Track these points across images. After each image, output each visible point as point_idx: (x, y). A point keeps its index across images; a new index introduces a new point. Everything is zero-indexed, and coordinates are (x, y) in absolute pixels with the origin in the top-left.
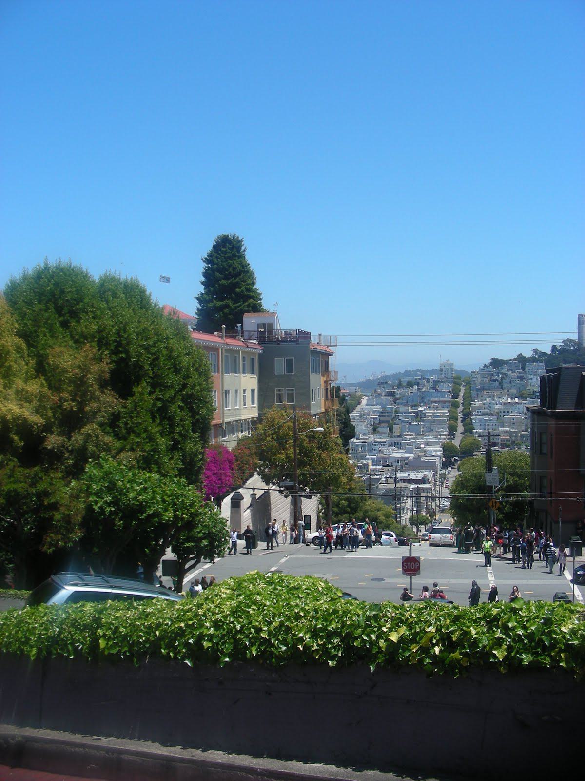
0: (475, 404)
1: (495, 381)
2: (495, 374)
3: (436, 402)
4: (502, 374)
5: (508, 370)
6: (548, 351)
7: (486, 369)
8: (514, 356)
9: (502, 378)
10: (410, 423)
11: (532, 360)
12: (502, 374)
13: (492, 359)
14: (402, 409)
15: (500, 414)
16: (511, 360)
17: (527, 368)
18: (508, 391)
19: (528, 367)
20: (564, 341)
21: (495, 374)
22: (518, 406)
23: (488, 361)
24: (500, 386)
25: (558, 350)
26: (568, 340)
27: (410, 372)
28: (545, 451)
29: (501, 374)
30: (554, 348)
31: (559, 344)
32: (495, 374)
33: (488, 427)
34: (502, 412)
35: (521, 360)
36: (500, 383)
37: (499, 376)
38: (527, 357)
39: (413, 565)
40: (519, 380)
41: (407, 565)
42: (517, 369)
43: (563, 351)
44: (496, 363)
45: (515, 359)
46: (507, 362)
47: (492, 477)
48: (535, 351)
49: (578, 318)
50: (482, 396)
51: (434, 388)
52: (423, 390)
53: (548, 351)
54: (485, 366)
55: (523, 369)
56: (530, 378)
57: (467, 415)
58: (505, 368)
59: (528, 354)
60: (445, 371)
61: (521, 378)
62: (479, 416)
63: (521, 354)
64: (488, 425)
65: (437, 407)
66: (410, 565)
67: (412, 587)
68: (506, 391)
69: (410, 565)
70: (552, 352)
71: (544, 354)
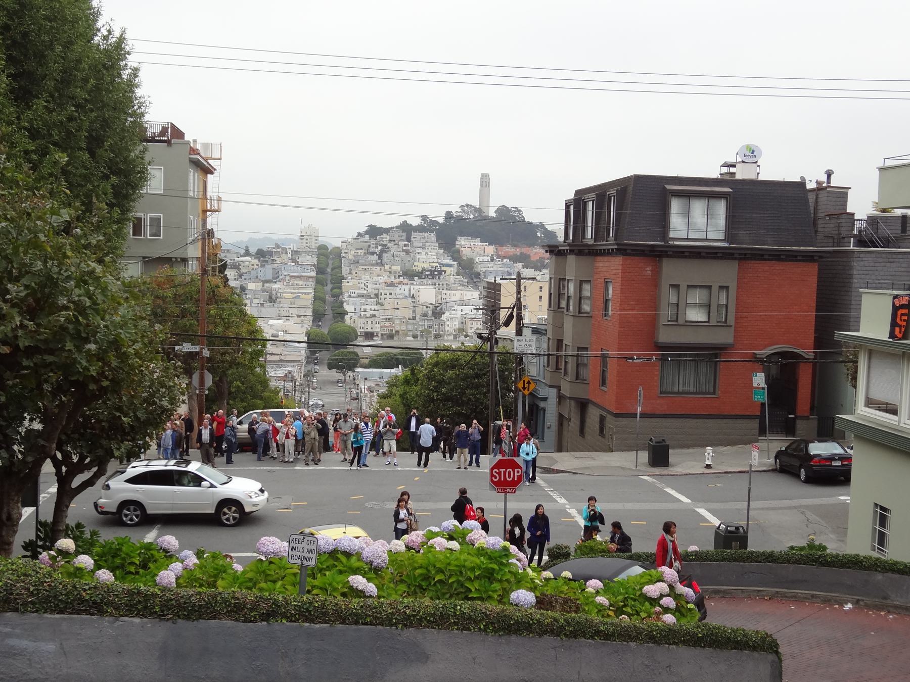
0: (348, 282)
1: (373, 254)
2: (374, 246)
3: (296, 277)
4: (382, 245)
5: (390, 241)
6: (441, 221)
7: (361, 239)
8: (395, 222)
9: (382, 252)
11: (420, 229)
12: (382, 245)
13: (369, 226)
14: (251, 286)
15: (380, 297)
16: (392, 228)
17: (413, 240)
18: (390, 268)
19: (417, 237)
20: (462, 206)
21: (372, 246)
24: (379, 261)
25: (454, 218)
26: (467, 205)
28: (586, 307)
30: (449, 215)
31: (455, 210)
32: (374, 246)
34: (383, 294)
35: (406, 229)
36: (380, 257)
37: (377, 248)
38: (414, 225)
39: (510, 472)
40: (405, 253)
41: (499, 473)
42: (401, 240)
43: (459, 219)
44: (374, 231)
45: (397, 227)
46: (387, 231)
47: (524, 343)
48: (424, 218)
49: (481, 179)
50: (356, 273)
51: (293, 260)
54: (359, 234)
55: (408, 239)
56: (417, 251)
57: (337, 295)
58: (386, 238)
59: (415, 222)
60: (307, 240)
61: (407, 252)
62: (354, 297)
63: (406, 221)
66: (505, 472)
67: (747, 503)
68: (387, 267)
69: (505, 472)
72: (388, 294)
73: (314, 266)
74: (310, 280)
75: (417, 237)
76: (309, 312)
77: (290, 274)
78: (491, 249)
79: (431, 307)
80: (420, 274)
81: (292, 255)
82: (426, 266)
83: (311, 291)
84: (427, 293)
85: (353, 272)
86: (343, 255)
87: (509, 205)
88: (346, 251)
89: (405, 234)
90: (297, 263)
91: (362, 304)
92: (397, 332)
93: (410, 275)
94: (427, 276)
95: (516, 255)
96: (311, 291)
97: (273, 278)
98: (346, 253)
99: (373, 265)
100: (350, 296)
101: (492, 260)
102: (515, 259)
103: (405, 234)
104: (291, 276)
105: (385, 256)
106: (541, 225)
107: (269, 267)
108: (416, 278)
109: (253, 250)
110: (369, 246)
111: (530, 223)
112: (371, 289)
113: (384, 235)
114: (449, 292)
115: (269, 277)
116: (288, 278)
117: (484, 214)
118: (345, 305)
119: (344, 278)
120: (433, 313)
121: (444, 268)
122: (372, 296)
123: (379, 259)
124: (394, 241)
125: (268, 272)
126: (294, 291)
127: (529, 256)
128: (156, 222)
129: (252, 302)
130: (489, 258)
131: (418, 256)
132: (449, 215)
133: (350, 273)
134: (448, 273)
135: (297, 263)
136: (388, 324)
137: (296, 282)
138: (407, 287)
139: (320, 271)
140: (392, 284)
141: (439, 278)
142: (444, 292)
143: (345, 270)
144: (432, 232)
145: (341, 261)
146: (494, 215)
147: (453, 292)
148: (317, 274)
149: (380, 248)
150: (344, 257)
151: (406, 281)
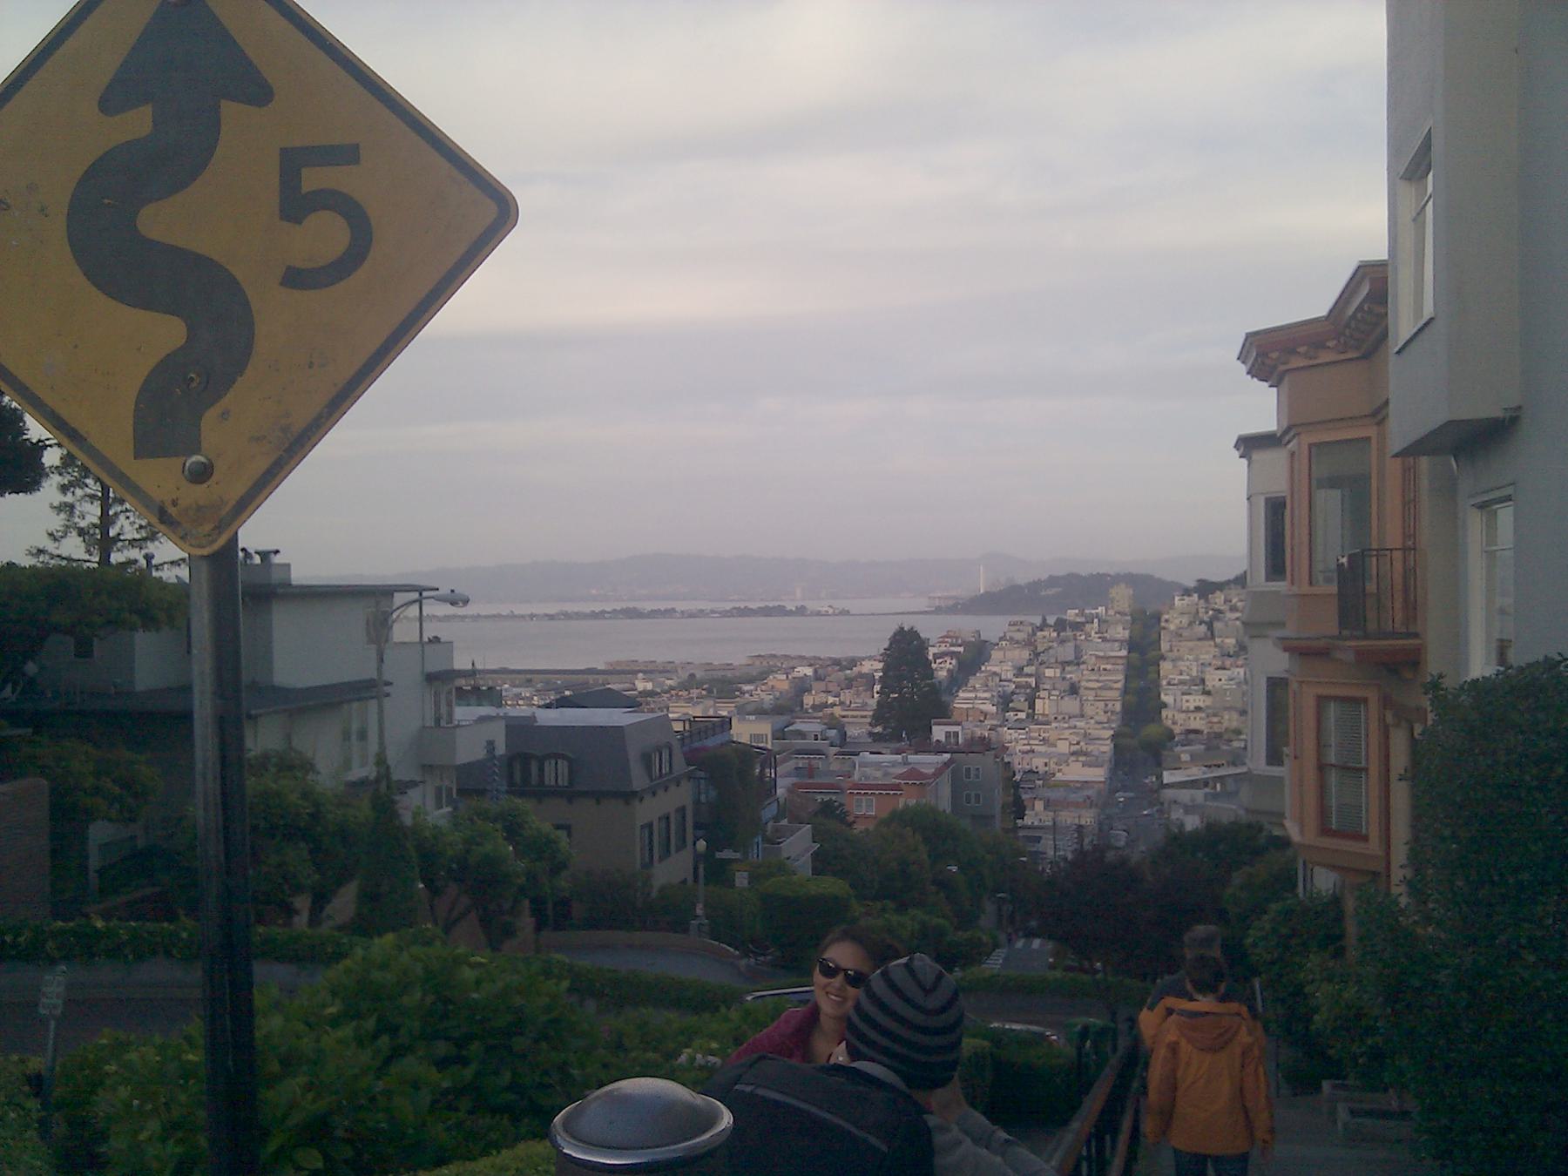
9: (1214, 618)
13: (1199, 581)
16: (1228, 582)
22: (1238, 670)
23: (1192, 584)
24: (1209, 633)
27: (1058, 578)
29: (1213, 609)
33: (1188, 704)
37: (1207, 613)
44: (1205, 589)
46: (1220, 586)
50: (1178, 650)
58: (1218, 599)
62: (1174, 685)
64: (1187, 701)
65: (1105, 669)
68: (1218, 640)
72: (1217, 680)
73: (1125, 641)
74: (1120, 661)
76: (1118, 707)
77: (1097, 653)
81: (1099, 625)
83: (1121, 677)
85: (1175, 650)
86: (1163, 624)
88: (1166, 617)
91: (1183, 694)
96: (1119, 678)
97: (1076, 658)
98: (1167, 621)
99: (1200, 639)
100: (1169, 684)
104: (1097, 657)
105: (1217, 625)
107: (1071, 645)
109: (1051, 620)
110: (1197, 610)
115: (1071, 657)
116: (1094, 658)
118: (1163, 696)
123: (1208, 629)
126: (1101, 678)
128: (977, 796)
129: (1050, 695)
133: (1171, 651)
137: (1103, 667)
139: (1132, 645)
143: (1165, 646)
148: (1129, 652)
150: (1164, 628)
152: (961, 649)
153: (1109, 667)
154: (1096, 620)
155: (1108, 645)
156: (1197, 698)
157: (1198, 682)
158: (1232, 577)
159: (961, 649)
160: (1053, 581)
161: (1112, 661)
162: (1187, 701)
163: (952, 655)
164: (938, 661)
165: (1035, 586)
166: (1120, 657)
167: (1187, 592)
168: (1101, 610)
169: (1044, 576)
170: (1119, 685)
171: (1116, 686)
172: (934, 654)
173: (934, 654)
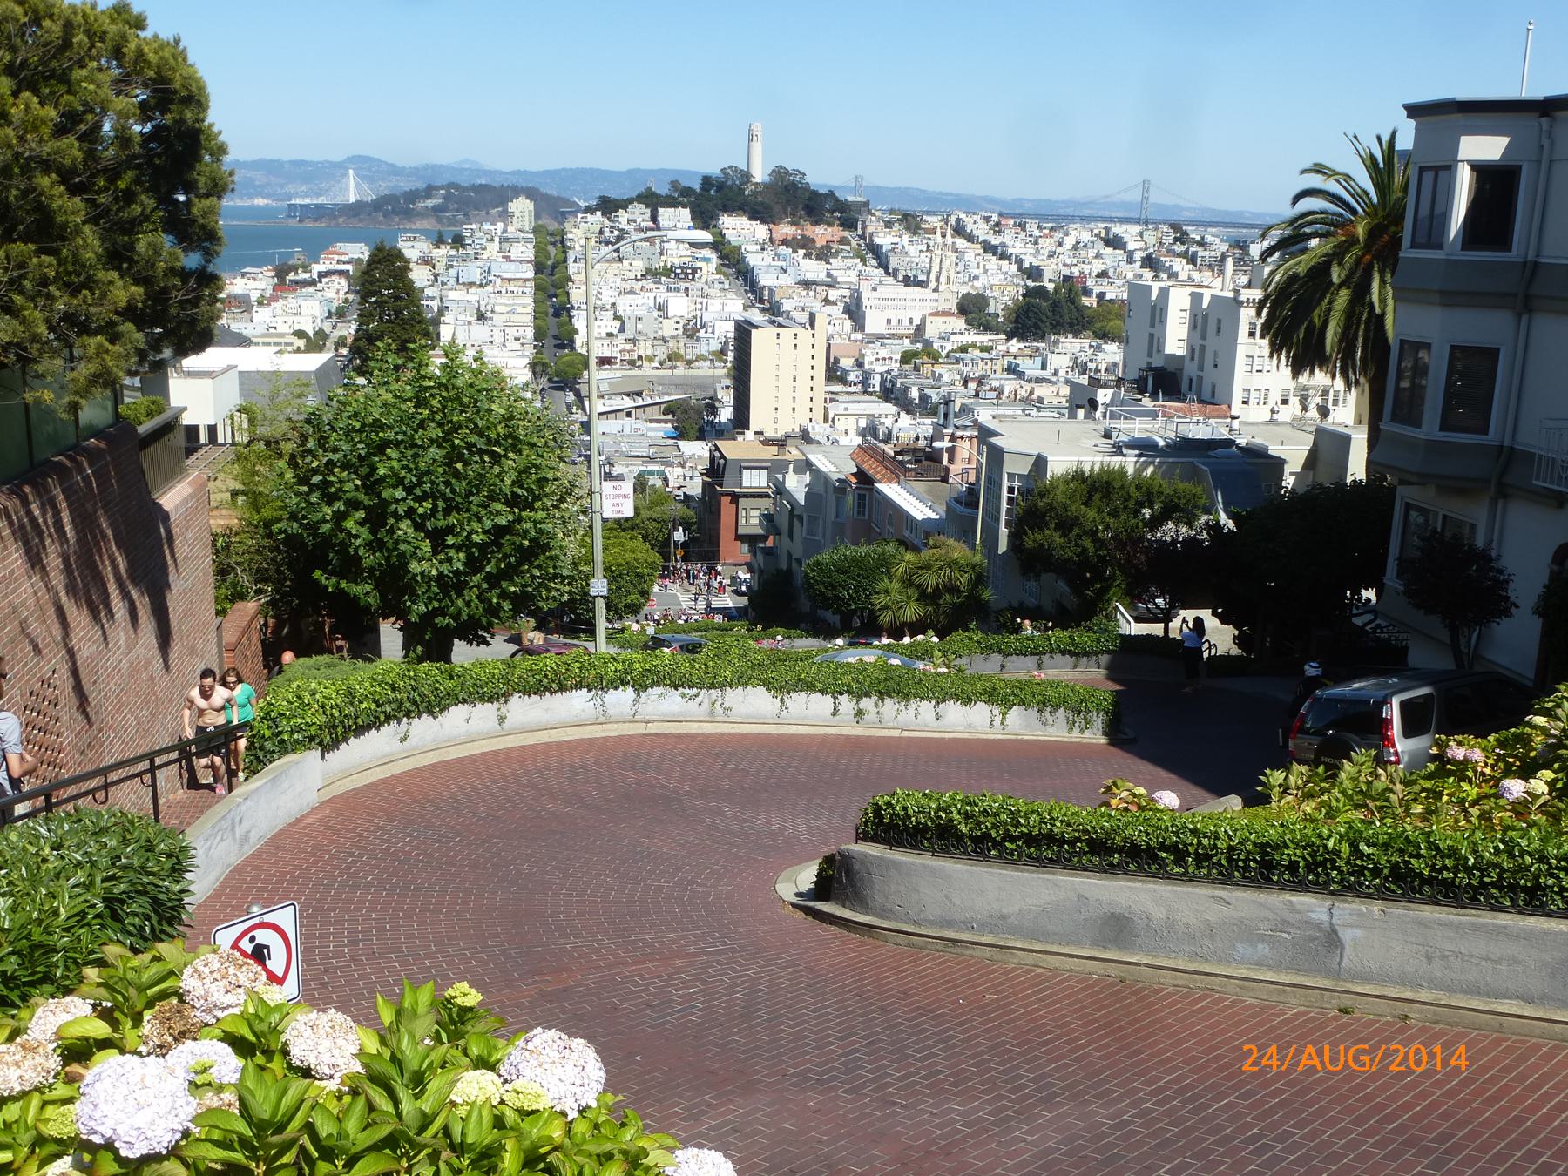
3: (509, 280)
4: (619, 230)
5: (629, 221)
6: (697, 186)
9: (619, 239)
10: (470, 323)
20: (723, 170)
23: (594, 202)
26: (731, 167)
27: (438, 188)
35: (652, 200)
43: (721, 186)
48: (674, 184)
52: (484, 257)
53: (697, 186)
55: (654, 218)
58: (623, 217)
59: (663, 190)
70: (702, 189)
71: (687, 192)
74: (528, 284)
75: (665, 214)
76: (530, 333)
78: (762, 231)
79: (682, 322)
80: (669, 271)
82: (677, 262)
83: (529, 300)
84: (680, 306)
87: (790, 167)
89: (649, 210)
90: (508, 259)
92: (640, 357)
93: (653, 273)
94: (677, 275)
95: (794, 238)
101: (763, 249)
102: (793, 243)
103: (649, 210)
106: (831, 194)
108: (663, 279)
111: (815, 193)
112: (608, 296)
113: (621, 212)
114: (705, 300)
115: (477, 278)
116: (498, 281)
117: (754, 180)
119: (570, 279)
120: (685, 330)
121: (698, 264)
122: (608, 307)
124: (634, 221)
125: (472, 272)
127: (813, 241)
130: (759, 247)
131: (666, 245)
132: (707, 181)
134: (704, 271)
135: (508, 259)
136: (629, 347)
138: (651, 295)
139: (539, 268)
140: (632, 292)
141: (693, 279)
142: (699, 300)
143: (572, 268)
144: (684, 207)
145: (565, 252)
146: (767, 179)
147: (710, 301)
149: (616, 233)
151: (648, 284)
152: (349, 267)
153: (516, 290)
154: (497, 238)
155: (512, 266)
156: (609, 324)
157: (608, 307)
158: (634, 195)
159: (349, 267)
160: (429, 191)
161: (520, 283)
162: (599, 327)
163: (341, 273)
164: (324, 280)
165: (413, 196)
166: (526, 280)
167: (589, 210)
168: (500, 226)
169: (421, 185)
170: (530, 309)
171: (524, 310)
172: (320, 273)
173: (320, 273)
